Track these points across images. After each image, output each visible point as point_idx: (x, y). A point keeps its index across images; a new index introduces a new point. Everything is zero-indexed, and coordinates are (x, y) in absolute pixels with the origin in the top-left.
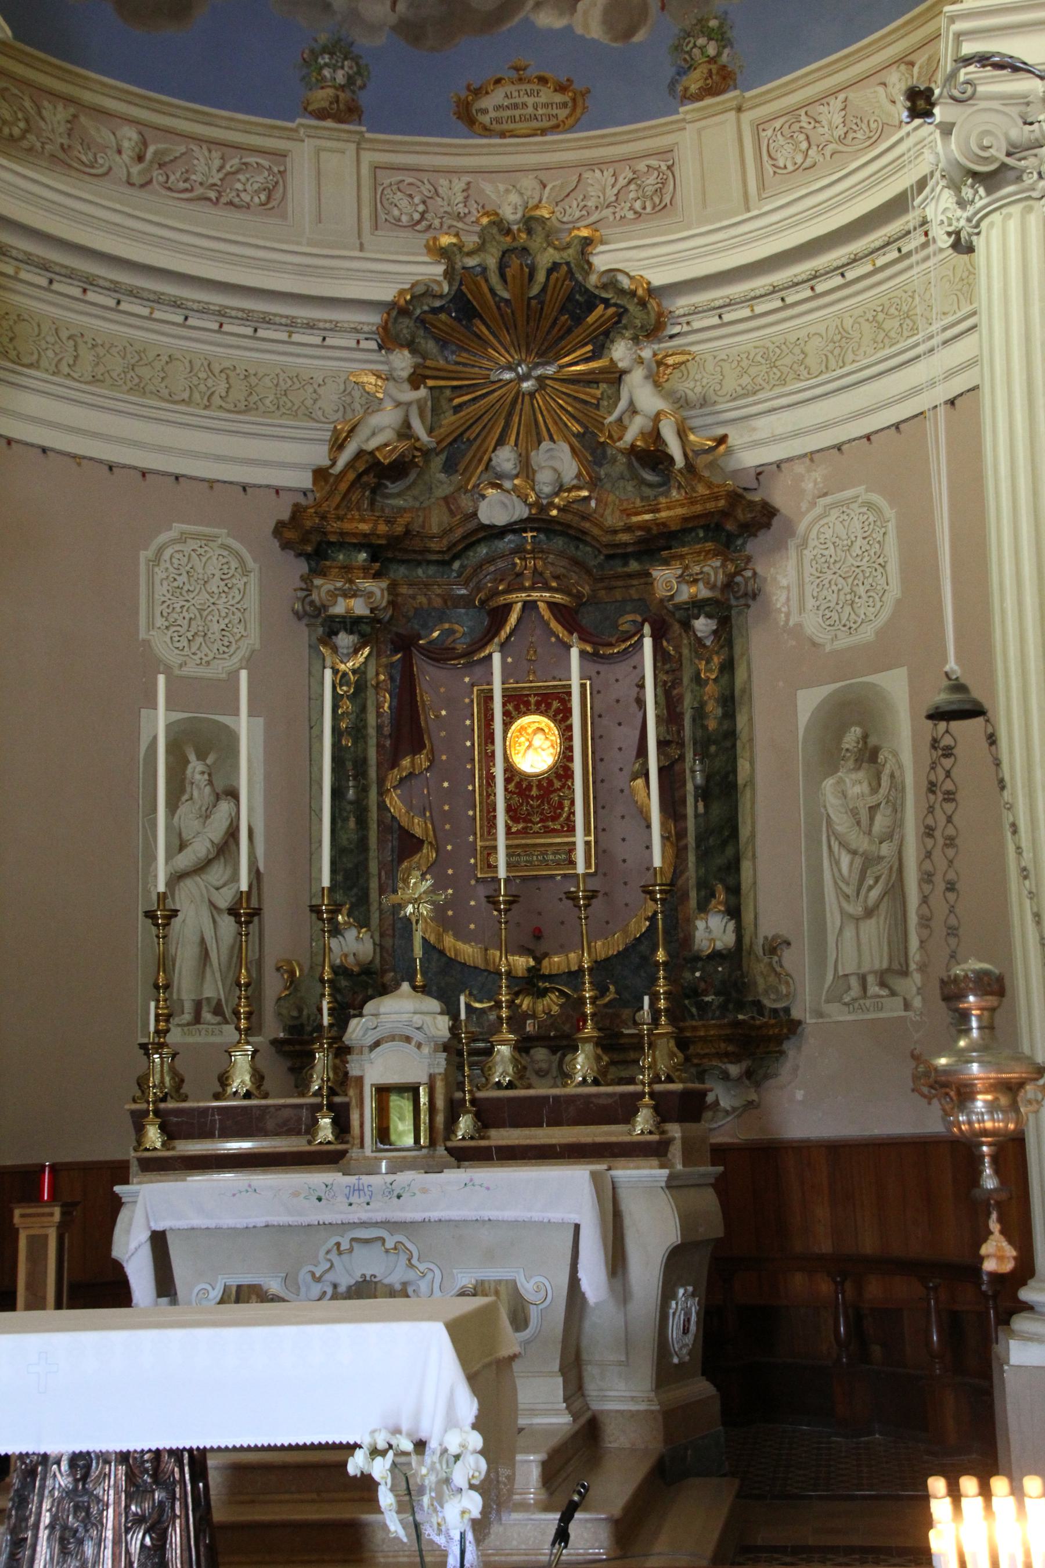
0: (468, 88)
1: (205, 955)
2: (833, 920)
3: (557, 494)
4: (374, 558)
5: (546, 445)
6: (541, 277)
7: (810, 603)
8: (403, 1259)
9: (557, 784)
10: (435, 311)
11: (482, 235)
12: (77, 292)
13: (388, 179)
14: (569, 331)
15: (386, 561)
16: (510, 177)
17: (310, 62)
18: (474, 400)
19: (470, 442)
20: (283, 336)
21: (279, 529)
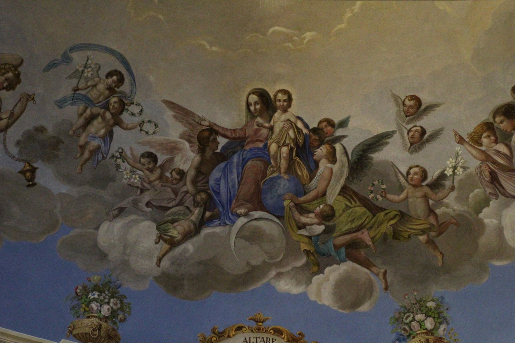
17: (82, 297)
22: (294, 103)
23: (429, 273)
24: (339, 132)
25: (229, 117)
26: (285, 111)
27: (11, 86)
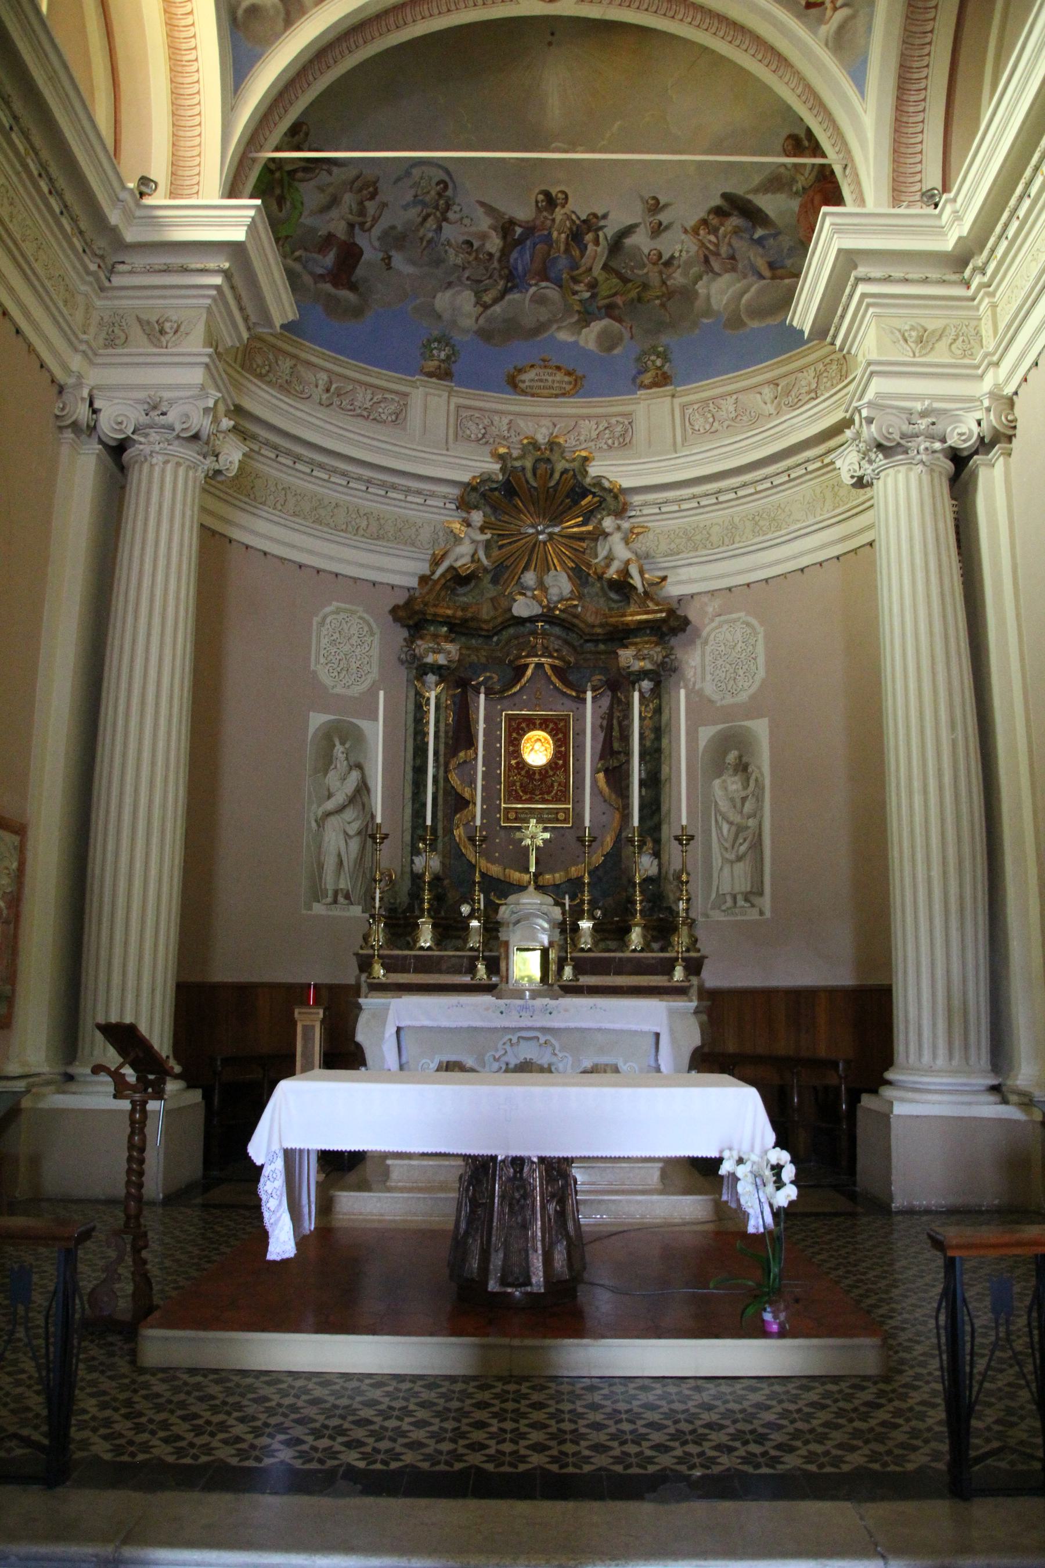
1: (341, 863)
2: (717, 862)
3: (559, 602)
4: (451, 631)
5: (552, 572)
6: (557, 476)
7: (709, 677)
8: (550, 1050)
9: (551, 773)
10: (492, 490)
11: (523, 449)
12: (290, 463)
13: (464, 413)
14: (570, 508)
15: (457, 634)
16: (535, 418)
18: (510, 543)
19: (507, 567)
20: (401, 497)
21: (394, 611)
22: (570, 200)
23: (661, 327)
24: (602, 223)
25: (523, 212)
26: (563, 206)
27: (373, 196)
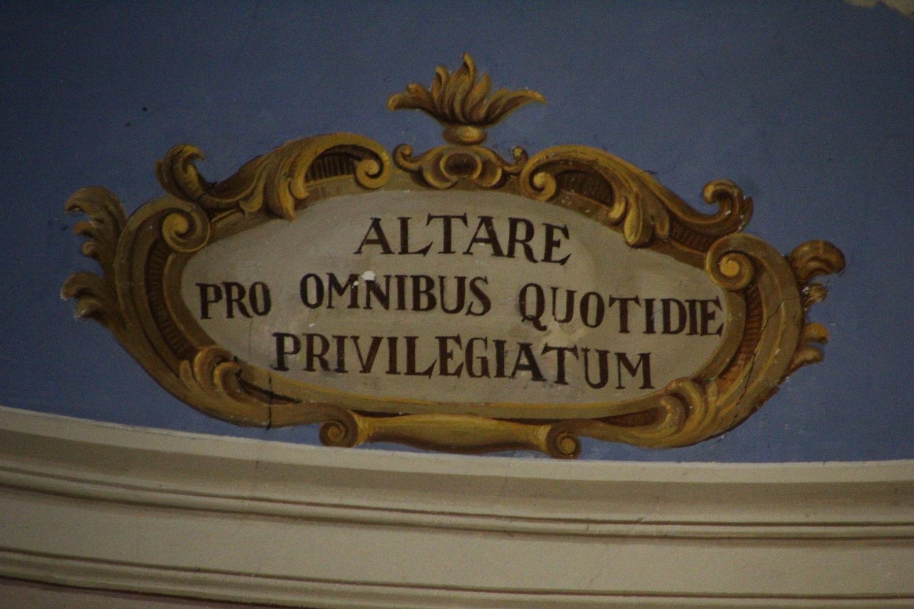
0: (171, 177)
